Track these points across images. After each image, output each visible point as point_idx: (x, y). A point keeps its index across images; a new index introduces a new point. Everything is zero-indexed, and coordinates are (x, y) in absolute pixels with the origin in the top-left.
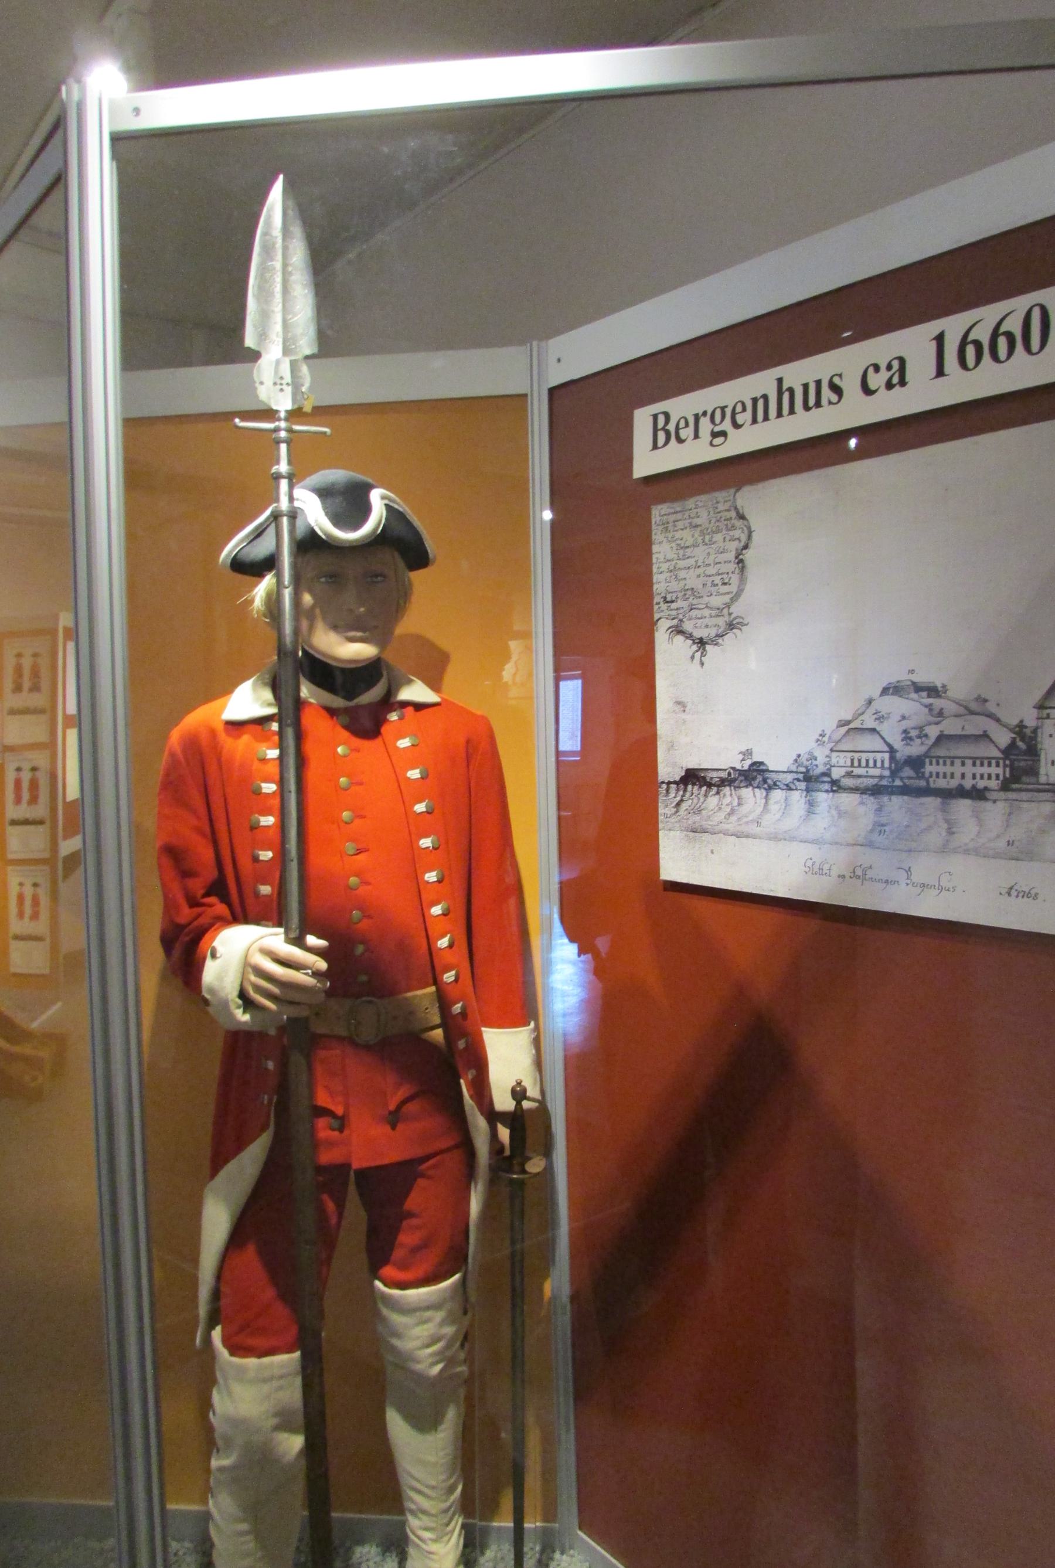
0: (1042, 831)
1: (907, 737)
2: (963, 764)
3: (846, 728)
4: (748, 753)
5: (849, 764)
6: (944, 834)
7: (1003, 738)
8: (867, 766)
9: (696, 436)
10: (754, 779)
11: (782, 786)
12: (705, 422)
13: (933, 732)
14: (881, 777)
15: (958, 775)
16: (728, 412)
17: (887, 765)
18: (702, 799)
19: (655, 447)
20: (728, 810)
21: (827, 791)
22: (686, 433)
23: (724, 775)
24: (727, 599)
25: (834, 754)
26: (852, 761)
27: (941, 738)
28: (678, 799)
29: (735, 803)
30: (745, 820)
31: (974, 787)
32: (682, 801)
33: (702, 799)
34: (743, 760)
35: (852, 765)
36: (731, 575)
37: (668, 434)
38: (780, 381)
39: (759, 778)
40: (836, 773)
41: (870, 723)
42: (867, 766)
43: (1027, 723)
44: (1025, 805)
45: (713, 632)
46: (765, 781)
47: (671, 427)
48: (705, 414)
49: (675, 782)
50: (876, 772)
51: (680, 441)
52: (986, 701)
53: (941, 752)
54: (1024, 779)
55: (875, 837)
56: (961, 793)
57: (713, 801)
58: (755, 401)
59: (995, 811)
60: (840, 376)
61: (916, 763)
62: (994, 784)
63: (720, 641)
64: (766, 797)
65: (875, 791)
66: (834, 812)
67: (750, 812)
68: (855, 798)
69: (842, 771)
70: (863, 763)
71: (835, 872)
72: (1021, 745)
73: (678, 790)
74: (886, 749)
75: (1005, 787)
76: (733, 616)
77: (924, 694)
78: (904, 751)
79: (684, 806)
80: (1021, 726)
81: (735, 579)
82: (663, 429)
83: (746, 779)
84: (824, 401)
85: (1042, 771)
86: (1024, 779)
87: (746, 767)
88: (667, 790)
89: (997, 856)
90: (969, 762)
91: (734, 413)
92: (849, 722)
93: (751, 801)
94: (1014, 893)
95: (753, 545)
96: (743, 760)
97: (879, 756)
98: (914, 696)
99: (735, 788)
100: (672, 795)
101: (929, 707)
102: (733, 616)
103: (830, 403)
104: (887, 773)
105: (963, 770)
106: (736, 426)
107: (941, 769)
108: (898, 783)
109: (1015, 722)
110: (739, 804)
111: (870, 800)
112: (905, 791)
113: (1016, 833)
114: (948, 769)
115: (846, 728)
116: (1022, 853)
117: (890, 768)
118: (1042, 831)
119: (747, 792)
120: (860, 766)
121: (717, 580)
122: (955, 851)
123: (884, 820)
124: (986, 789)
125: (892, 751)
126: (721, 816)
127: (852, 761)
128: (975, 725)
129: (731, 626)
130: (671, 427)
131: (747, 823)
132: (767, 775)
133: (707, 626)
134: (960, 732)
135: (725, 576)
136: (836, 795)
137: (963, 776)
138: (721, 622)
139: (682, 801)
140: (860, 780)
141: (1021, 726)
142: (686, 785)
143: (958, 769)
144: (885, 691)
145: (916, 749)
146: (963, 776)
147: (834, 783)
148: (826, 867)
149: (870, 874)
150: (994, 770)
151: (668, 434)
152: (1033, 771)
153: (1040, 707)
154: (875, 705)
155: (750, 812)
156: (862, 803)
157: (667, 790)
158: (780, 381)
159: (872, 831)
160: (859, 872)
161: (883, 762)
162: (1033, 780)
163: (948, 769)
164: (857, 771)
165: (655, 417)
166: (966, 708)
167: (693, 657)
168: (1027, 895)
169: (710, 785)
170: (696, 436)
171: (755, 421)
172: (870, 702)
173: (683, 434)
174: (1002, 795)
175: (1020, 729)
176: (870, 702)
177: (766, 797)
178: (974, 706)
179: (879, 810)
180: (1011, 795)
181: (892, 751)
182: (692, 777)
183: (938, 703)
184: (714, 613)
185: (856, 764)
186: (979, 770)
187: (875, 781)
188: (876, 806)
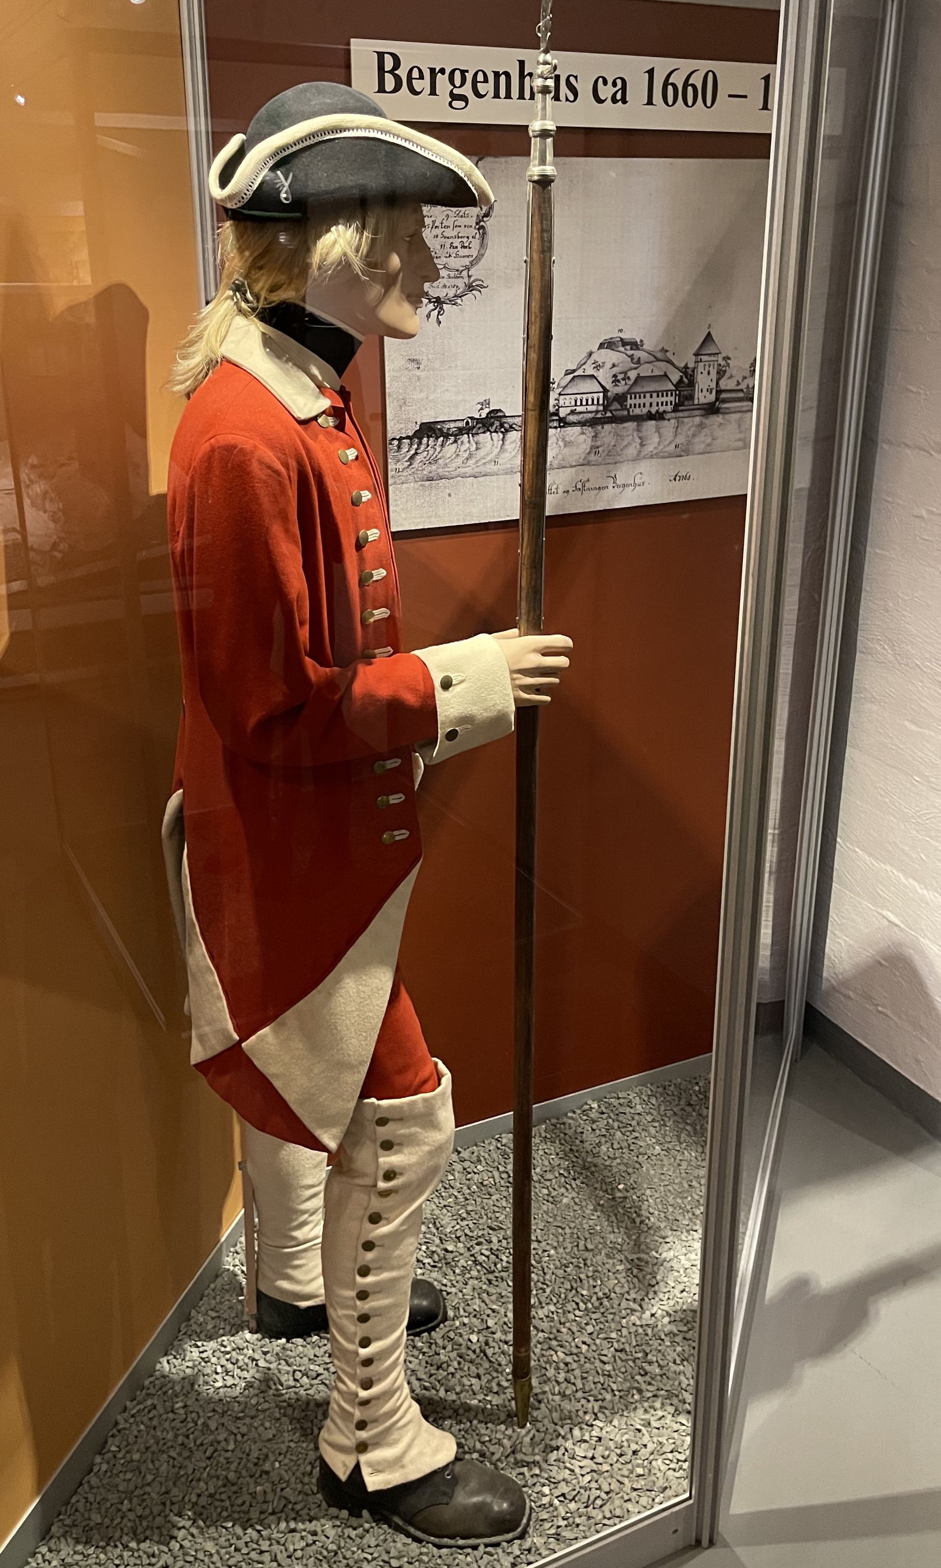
0: (694, 435)
1: (616, 381)
2: (651, 397)
3: (572, 376)
4: (487, 403)
5: (573, 403)
6: (638, 446)
7: (675, 376)
8: (587, 404)
9: (433, 92)
10: (492, 424)
11: (517, 428)
12: (442, 80)
13: (633, 375)
14: (597, 412)
15: (648, 405)
16: (469, 77)
17: (601, 402)
18: (438, 449)
19: (381, 89)
20: (466, 455)
21: (556, 428)
22: (421, 85)
23: (460, 424)
24: (467, 261)
25: (562, 397)
26: (576, 401)
27: (639, 378)
28: (412, 452)
29: (474, 447)
30: (484, 461)
31: (657, 411)
32: (416, 453)
33: (438, 449)
34: (482, 409)
35: (576, 405)
36: (471, 239)
37: (398, 80)
38: (522, 63)
39: (497, 423)
40: (563, 413)
41: (590, 371)
42: (587, 404)
43: (689, 366)
44: (686, 420)
45: (451, 293)
46: (502, 425)
47: (402, 73)
48: (442, 71)
49: (408, 437)
50: (594, 408)
51: (414, 92)
52: (667, 351)
53: (638, 389)
54: (686, 403)
55: (592, 457)
56: (650, 417)
57: (450, 449)
58: (497, 75)
59: (668, 426)
60: (576, 77)
61: (621, 399)
62: (669, 408)
63: (459, 301)
64: (503, 440)
65: (593, 423)
66: (561, 443)
67: (488, 454)
68: (577, 429)
69: (568, 410)
70: (584, 403)
71: (560, 491)
72: (685, 380)
73: (411, 445)
74: (601, 390)
75: (675, 410)
76: (472, 279)
77: (628, 347)
78: (614, 390)
79: (419, 458)
80: (686, 367)
81: (475, 244)
82: (391, 72)
83: (484, 426)
84: (562, 97)
85: (696, 397)
86: (686, 403)
87: (484, 416)
88: (399, 447)
89: (670, 456)
90: (655, 395)
91: (475, 82)
92: (574, 371)
93: (489, 445)
94: (678, 478)
95: (493, 214)
96: (482, 409)
97: (595, 396)
98: (622, 349)
99: (473, 435)
100: (405, 450)
101: (631, 357)
102: (472, 279)
103: (567, 100)
104: (601, 408)
105: (651, 400)
106: (479, 95)
107: (637, 401)
108: (609, 414)
109: (682, 365)
110: (477, 449)
111: (589, 431)
112: (614, 420)
113: (681, 439)
114: (642, 401)
115: (572, 376)
116: (683, 451)
117: (603, 404)
118: (694, 435)
119: (484, 438)
120: (593, 404)
121: (457, 242)
122: (644, 458)
123: (598, 443)
124: (664, 411)
125: (605, 391)
126: (459, 461)
127: (576, 401)
128: (659, 368)
129: (470, 288)
130: (402, 73)
131: (484, 464)
132: (504, 420)
133: (445, 286)
134: (650, 374)
135: (465, 240)
136: (563, 429)
137: (651, 404)
138: (461, 283)
139: (416, 453)
140: (581, 416)
141: (686, 367)
142: (420, 439)
143: (648, 400)
144: (601, 346)
145: (621, 389)
146: (651, 404)
147: (561, 420)
148: (555, 486)
149: (587, 485)
150: (670, 399)
151: (398, 80)
152: (691, 397)
153: (696, 354)
154: (594, 357)
155: (488, 454)
156: (583, 433)
157: (399, 447)
158: (522, 63)
159: (589, 453)
160: (579, 486)
161: (598, 400)
162: (691, 403)
163: (642, 401)
164: (579, 409)
165: (381, 55)
166: (655, 357)
167: (428, 316)
168: (685, 478)
169: (446, 436)
170: (433, 92)
171: (497, 95)
172: (590, 354)
173: (417, 85)
174: (673, 414)
175: (685, 370)
176: (590, 354)
177: (503, 440)
178: (659, 355)
179: (595, 436)
180: (680, 414)
181: (605, 391)
182: (429, 430)
183: (637, 354)
184: (452, 274)
185: (579, 403)
186: (661, 399)
187: (590, 416)
188: (593, 434)
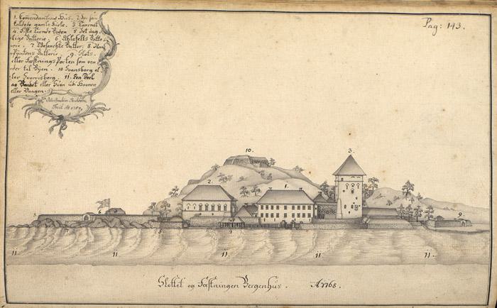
1: (244, 192)
2: (286, 208)
3: (196, 185)
4: (107, 202)
5: (198, 208)
6: (272, 252)
7: (313, 192)
8: (213, 210)
11: (138, 226)
13: (264, 188)
15: (281, 215)
17: (228, 209)
18: (56, 238)
20: (84, 245)
23: (79, 219)
25: (185, 203)
26: (200, 206)
27: (270, 191)
28: (30, 238)
29: (92, 239)
30: (102, 252)
33: (56, 238)
34: (101, 207)
35: (200, 210)
40: (187, 216)
41: (215, 182)
42: (213, 210)
44: (326, 232)
45: (74, 112)
49: (28, 226)
50: (221, 214)
53: (269, 201)
55: (219, 257)
56: (285, 226)
57: (68, 239)
61: (251, 208)
62: (307, 220)
63: (81, 119)
68: (204, 232)
69: (192, 214)
70: (210, 208)
77: (258, 165)
78: (242, 200)
79: (36, 244)
87: (103, 212)
89: (311, 263)
90: (290, 207)
92: (198, 181)
94: (320, 285)
96: (101, 207)
97: (222, 204)
98: (252, 166)
101: (262, 174)
104: (229, 215)
107: (270, 211)
108: (237, 221)
109: (320, 183)
110: (95, 241)
112: (242, 226)
114: (275, 211)
117: (231, 212)
119: (104, 232)
122: (279, 263)
123: (226, 246)
124: (302, 223)
125: (233, 200)
126: (76, 250)
127: (200, 206)
128: (294, 185)
132: (123, 218)
133: (68, 107)
134: (283, 188)
136: (186, 230)
137: (285, 215)
139: (34, 240)
140: (208, 220)
143: (282, 211)
144: (228, 162)
145: (251, 199)
146: (285, 215)
147: (184, 222)
149: (214, 282)
150: (307, 211)
154: (220, 170)
155: (107, 246)
156: (208, 235)
157: (17, 234)
161: (225, 207)
162: (334, 217)
163: (275, 211)
166: (288, 174)
169: (65, 227)
175: (324, 187)
176: (216, 168)
177: (123, 235)
178: (293, 173)
180: (318, 226)
182: (46, 221)
183: (268, 171)
188: (219, 237)
